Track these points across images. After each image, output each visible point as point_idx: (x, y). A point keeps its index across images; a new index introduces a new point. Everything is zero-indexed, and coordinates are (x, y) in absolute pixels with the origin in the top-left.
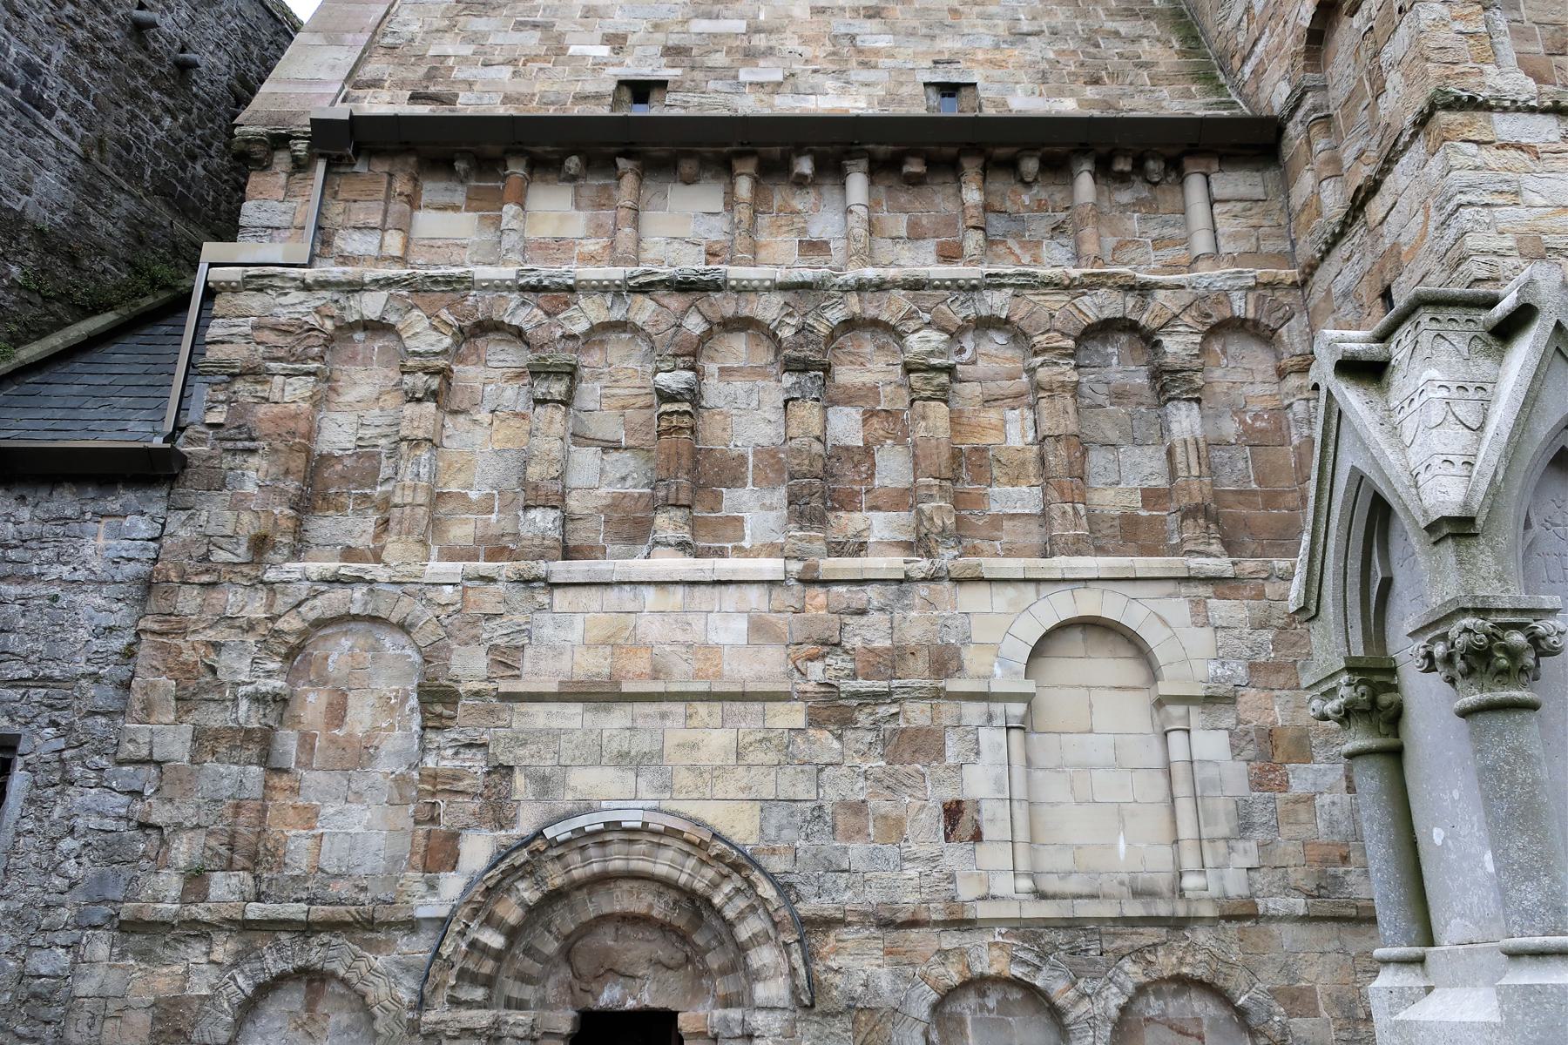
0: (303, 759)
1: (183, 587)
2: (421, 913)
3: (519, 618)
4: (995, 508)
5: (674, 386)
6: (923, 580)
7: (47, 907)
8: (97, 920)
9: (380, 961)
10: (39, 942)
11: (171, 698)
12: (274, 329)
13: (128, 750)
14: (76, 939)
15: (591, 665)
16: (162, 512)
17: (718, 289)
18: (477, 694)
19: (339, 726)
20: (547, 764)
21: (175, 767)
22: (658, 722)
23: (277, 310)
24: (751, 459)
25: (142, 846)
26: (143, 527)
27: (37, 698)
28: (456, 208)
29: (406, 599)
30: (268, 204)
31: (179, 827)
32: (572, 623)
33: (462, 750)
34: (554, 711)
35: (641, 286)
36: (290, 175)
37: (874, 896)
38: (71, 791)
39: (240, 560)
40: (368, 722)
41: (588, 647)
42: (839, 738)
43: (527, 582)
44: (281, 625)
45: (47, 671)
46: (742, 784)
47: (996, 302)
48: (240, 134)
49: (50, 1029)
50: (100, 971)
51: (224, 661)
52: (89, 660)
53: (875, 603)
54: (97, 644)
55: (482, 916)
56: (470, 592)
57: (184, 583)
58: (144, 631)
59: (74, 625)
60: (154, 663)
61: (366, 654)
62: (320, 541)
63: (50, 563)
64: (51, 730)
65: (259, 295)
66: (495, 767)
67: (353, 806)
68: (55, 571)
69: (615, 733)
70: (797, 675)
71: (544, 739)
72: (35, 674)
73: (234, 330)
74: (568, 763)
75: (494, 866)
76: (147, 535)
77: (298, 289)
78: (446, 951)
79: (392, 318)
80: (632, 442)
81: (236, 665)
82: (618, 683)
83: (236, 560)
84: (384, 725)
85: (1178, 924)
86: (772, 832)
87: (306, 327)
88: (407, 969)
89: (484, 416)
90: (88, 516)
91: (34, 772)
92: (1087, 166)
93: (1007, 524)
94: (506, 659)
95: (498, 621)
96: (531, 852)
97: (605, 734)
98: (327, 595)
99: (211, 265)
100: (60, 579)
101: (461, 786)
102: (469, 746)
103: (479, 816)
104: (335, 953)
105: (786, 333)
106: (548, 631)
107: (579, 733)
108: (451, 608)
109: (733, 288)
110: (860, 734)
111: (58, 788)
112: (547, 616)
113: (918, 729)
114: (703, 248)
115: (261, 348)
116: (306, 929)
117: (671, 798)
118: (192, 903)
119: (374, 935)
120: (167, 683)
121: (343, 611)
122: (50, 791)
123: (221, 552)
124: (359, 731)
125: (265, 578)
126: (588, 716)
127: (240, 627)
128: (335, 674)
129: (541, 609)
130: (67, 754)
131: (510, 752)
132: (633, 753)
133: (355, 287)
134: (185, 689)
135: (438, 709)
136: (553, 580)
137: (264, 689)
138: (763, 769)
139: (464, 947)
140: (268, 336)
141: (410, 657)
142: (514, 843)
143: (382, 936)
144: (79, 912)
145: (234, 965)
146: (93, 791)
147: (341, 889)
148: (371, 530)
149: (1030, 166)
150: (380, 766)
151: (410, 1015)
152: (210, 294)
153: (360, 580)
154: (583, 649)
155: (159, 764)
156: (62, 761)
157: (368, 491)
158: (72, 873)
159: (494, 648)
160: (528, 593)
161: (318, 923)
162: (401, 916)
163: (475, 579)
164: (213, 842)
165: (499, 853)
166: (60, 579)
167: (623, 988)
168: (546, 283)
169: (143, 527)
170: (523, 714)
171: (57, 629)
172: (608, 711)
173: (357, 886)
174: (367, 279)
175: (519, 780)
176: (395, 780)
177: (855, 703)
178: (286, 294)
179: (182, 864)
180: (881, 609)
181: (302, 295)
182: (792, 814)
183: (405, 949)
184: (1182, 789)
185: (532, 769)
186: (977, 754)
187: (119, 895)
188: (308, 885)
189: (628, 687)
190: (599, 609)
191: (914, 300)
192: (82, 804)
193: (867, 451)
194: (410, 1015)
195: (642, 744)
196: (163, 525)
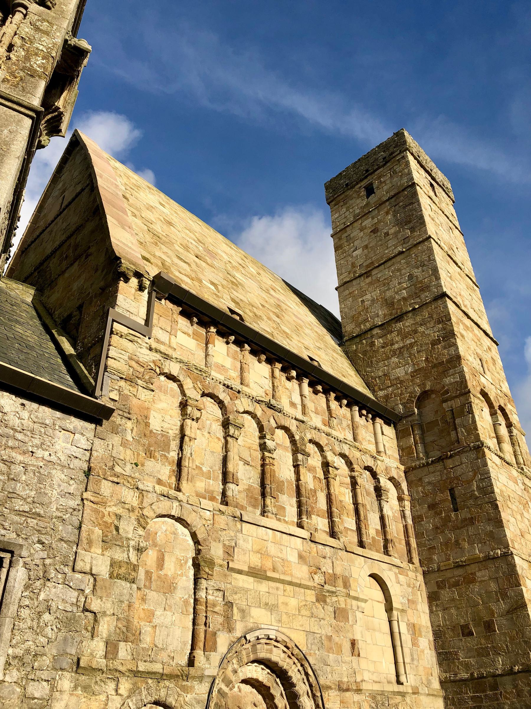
0: (147, 584)
1: (104, 481)
2: (207, 673)
3: (232, 534)
4: (346, 526)
5: (271, 447)
6: (340, 549)
7: (36, 655)
8: (65, 665)
9: (189, 697)
11: (100, 540)
12: (137, 362)
15: (256, 561)
16: (92, 437)
17: (280, 412)
18: (221, 566)
19: (161, 570)
20: (243, 604)
22: (275, 591)
23: (138, 354)
24: (286, 484)
27: (31, 525)
28: (189, 335)
31: (104, 614)
35: (259, 401)
37: (336, 678)
38: (49, 584)
41: (254, 552)
42: (323, 608)
43: (235, 517)
45: (38, 510)
46: (300, 623)
47: (346, 449)
50: (66, 697)
51: (122, 525)
52: (57, 509)
53: (328, 555)
54: (62, 501)
57: (104, 479)
58: (87, 499)
60: (92, 519)
61: (172, 535)
62: (148, 472)
64: (40, 546)
65: (131, 343)
68: (40, 453)
69: (264, 593)
70: (312, 579)
73: (121, 356)
74: (250, 605)
76: (85, 447)
77: (146, 347)
79: (181, 378)
80: (253, 464)
82: (265, 571)
84: (179, 573)
85: (403, 694)
86: (309, 645)
87: (149, 367)
89: (206, 434)
92: (357, 408)
93: (349, 532)
94: (229, 552)
97: (261, 593)
100: (43, 458)
101: (217, 609)
105: (297, 437)
106: (241, 542)
107: (253, 591)
109: (284, 413)
110: (329, 607)
111: (41, 581)
113: (343, 608)
114: (264, 390)
115: (131, 370)
116: (160, 677)
117: (282, 627)
120: (98, 532)
122: (38, 583)
127: (128, 509)
130: (48, 561)
132: (269, 604)
133: (167, 357)
134: (107, 536)
135: (207, 570)
138: (306, 618)
140: (133, 364)
141: (188, 541)
143: (189, 684)
146: (60, 586)
147: (163, 656)
148: (168, 473)
149: (345, 402)
153: (176, 498)
156: (44, 565)
157: (167, 454)
158: (50, 636)
161: (167, 675)
162: (199, 673)
164: (120, 626)
168: (233, 386)
169: (84, 443)
170: (235, 579)
171: (42, 486)
172: (261, 583)
173: (169, 656)
174: (174, 357)
177: (327, 594)
178: (141, 348)
179: (105, 636)
180: (330, 558)
181: (148, 352)
182: (314, 639)
183: (198, 692)
184: (398, 643)
186: (356, 621)
189: (270, 574)
191: (327, 439)
193: (315, 492)
195: (272, 601)
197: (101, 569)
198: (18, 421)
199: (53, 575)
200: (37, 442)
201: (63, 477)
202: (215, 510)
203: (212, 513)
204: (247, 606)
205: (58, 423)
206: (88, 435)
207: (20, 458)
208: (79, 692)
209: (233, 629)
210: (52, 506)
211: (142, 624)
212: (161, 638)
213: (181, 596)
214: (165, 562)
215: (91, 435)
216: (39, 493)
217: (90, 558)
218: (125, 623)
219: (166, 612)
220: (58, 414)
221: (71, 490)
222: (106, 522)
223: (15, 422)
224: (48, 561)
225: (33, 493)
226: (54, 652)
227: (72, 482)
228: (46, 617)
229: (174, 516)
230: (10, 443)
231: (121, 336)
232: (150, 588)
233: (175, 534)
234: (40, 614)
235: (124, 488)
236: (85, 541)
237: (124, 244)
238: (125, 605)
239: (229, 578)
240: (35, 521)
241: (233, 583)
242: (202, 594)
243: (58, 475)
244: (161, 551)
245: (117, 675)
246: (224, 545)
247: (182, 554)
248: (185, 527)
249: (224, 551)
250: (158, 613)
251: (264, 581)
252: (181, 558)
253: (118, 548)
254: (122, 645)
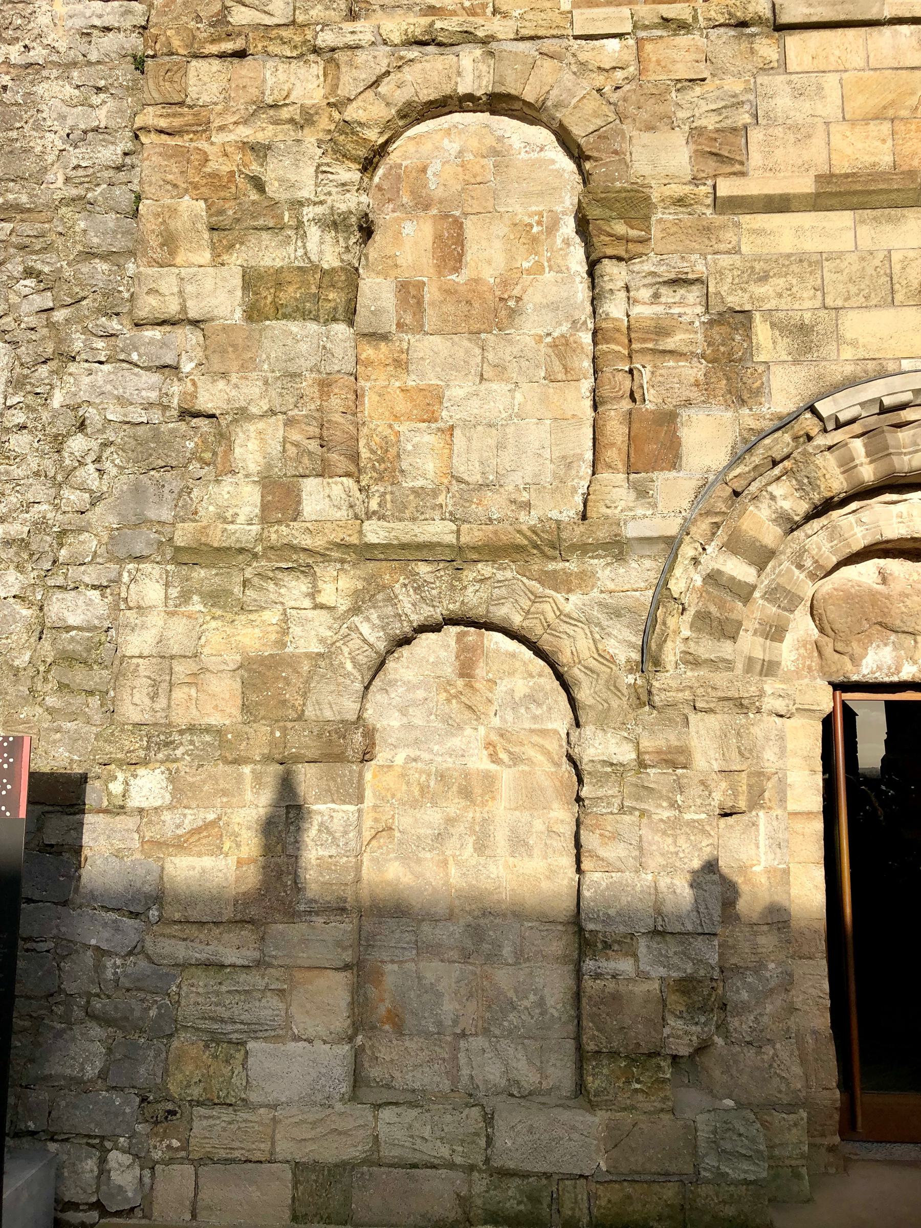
0: (408, 319)
1: (194, 63)
2: (632, 531)
3: (734, 85)
8: (140, 548)
9: (573, 603)
10: (60, 581)
11: (202, 226)
13: (148, 306)
14: (113, 575)
18: (680, 202)
19: (456, 270)
21: (225, 329)
25: (190, 445)
29: (548, 64)
31: (242, 415)
32: (820, 88)
33: (664, 290)
34: (807, 226)
38: (72, 368)
39: (276, 21)
40: (499, 260)
41: (853, 123)
43: (743, 24)
44: (352, 113)
45: (11, 197)
49: (95, 701)
50: (156, 620)
52: (67, 180)
55: (722, 535)
56: (649, 47)
57: (196, 56)
58: (145, 129)
59: (37, 127)
60: (170, 177)
61: (484, 161)
64: (31, 282)
66: (720, 314)
67: (494, 386)
69: (912, 254)
71: (795, 268)
74: (839, 303)
75: (737, 459)
78: (677, 586)
81: (292, 177)
83: (268, 20)
84: (526, 265)
88: (616, 613)
91: (15, 344)
95: (698, 90)
96: (796, 438)
97: (896, 257)
98: (417, 67)
101: (670, 343)
102: (676, 282)
103: (706, 386)
104: (503, 592)
107: (853, 258)
108: (619, 75)
111: (53, 365)
112: (780, 79)
118: (279, 522)
119: (561, 565)
121: (447, 90)
122: (43, 370)
123: (243, 9)
124: (489, 275)
125: (319, 42)
126: (865, 232)
127: (292, 121)
128: (439, 193)
129: (766, 69)
131: (744, 290)
134: (221, 212)
135: (620, 228)
136: (785, 19)
137: (343, 207)
139: (698, 581)
141: (553, 162)
142: (768, 425)
143: (572, 566)
144: (111, 538)
145: (356, 610)
146: (106, 368)
150: (528, 325)
151: (630, 679)
154: (845, 127)
155: (195, 323)
156: (50, 325)
159: (696, 133)
160: (744, 45)
161: (474, 548)
162: (602, 534)
163: (655, 26)
164: (295, 436)
165: (745, 441)
167: (895, 648)
171: (14, 134)
173: (513, 502)
175: (762, 331)
176: (554, 346)
179: (253, 468)
183: (611, 586)
185: (781, 315)
187: (166, 514)
188: (441, 499)
190: (862, 64)
192: (93, 386)
194: (630, 679)
197: (215, 302)
199: (78, 345)
201: (69, 91)
202: (646, 27)
203: (631, 42)
204: (823, 313)
208: (196, 605)
209: (757, 393)
210: (50, 177)
211: (403, 428)
212: (475, 457)
213: (541, 331)
214: (467, 246)
217: (174, 280)
218: (314, 430)
219: (485, 385)
221: (101, 117)
222: (214, 175)
226: (113, 521)
227: (96, 100)
228: (77, 444)
229: (470, 97)
232: (420, 329)
233: (495, 152)
234: (58, 442)
235: (270, 64)
236: (154, 241)
238: (307, 385)
239: (729, 235)
241: (744, 249)
242: (615, 309)
244: (447, 216)
245: (303, 558)
246: (696, 133)
247: (534, 208)
248: (533, 121)
249: (700, 154)
250: (456, 392)
251: (910, 213)
252: (527, 220)
253: (265, 235)
254: (310, 485)
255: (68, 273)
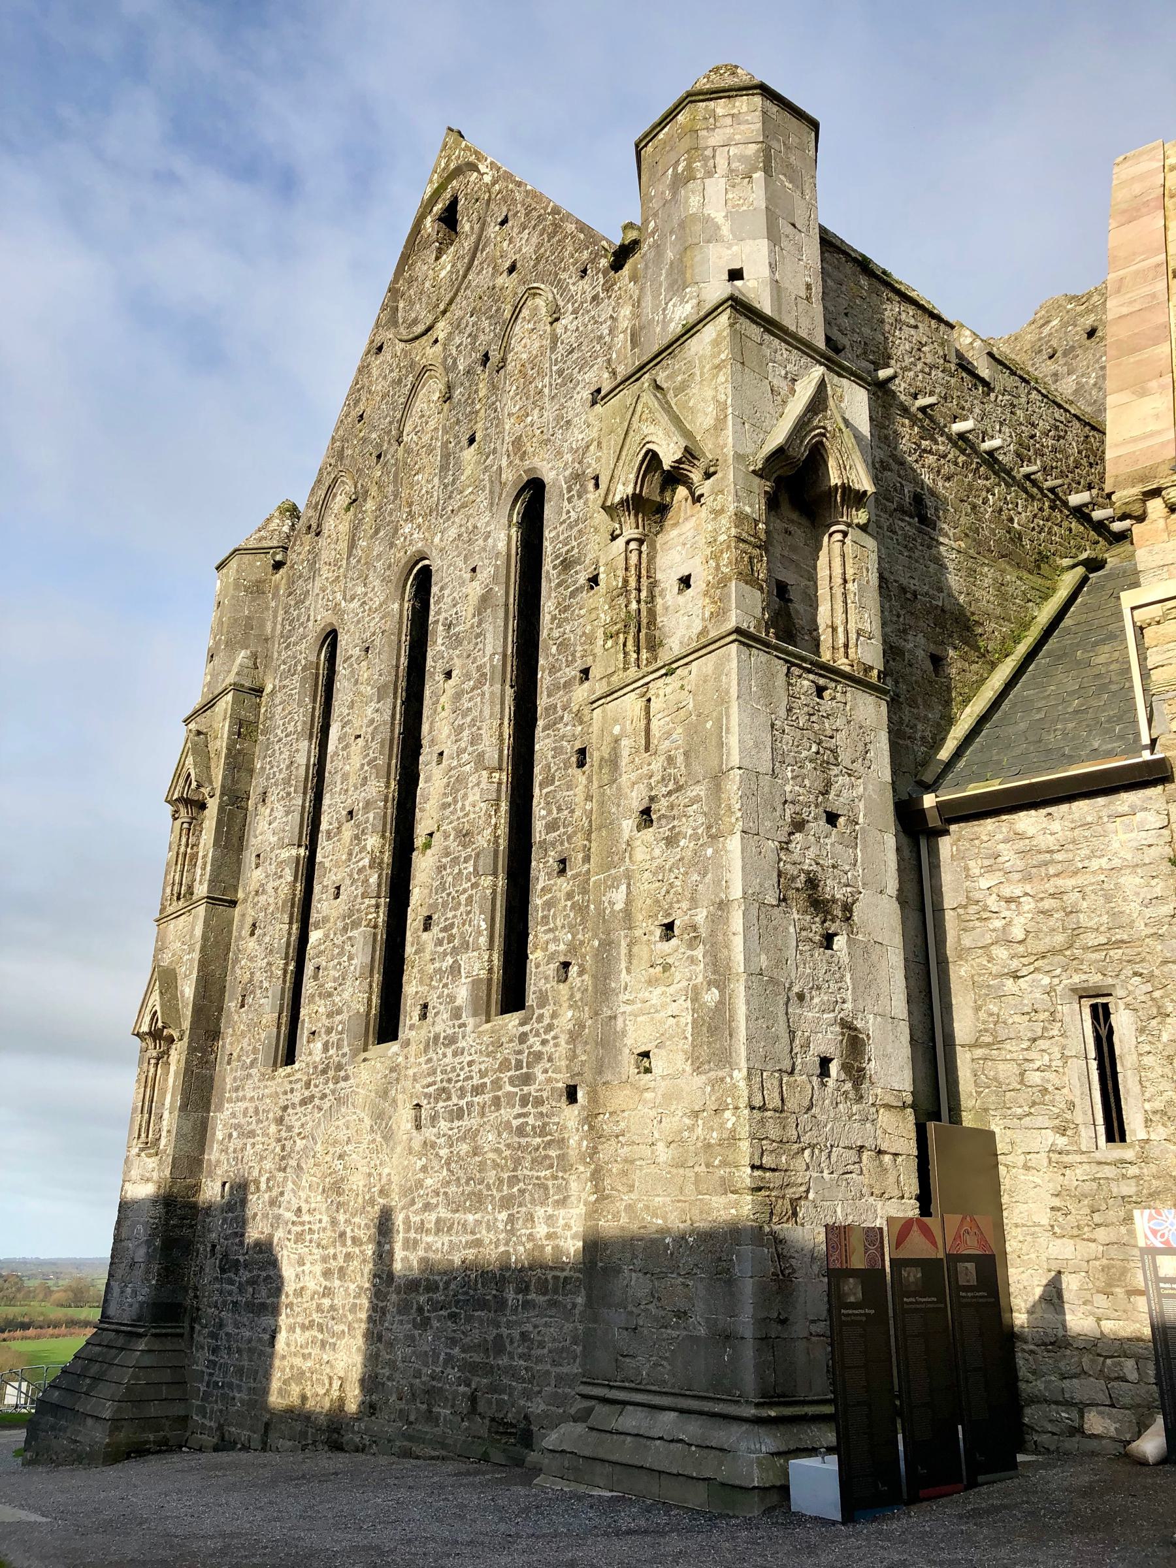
16: (1165, 806)
26: (1153, 819)
27: (1117, 957)
30: (1156, 548)
36: (1167, 518)
38: (1168, 1020)
45: (1118, 937)
48: (1120, 499)
54: (1148, 912)
63: (1089, 858)
68: (1095, 864)
72: (1109, 939)
90: (1105, 819)
99: (1133, 609)
100: (1101, 868)
111: (1159, 1019)
122: (1154, 1023)
130: (1157, 994)
152: (1140, 630)
156: (1153, 999)
166: (1101, 868)
169: (1154, 820)
171: (1112, 905)
196: (1168, 815)
198: (1051, 839)
200: (1085, 852)
201: (1138, 880)
205: (1104, 813)
206: (1155, 807)
207: (1070, 883)
210: (1137, 924)
215: (1160, 804)
216: (1113, 915)
220: (1101, 801)
221: (1158, 891)
223: (1050, 842)
224: (1157, 994)
225: (1105, 918)
227: (1153, 882)
230: (1052, 871)
231: (1158, 623)
237: (1134, 440)
240: (1120, 951)
243: (1130, 882)
255: (1157, 972)
